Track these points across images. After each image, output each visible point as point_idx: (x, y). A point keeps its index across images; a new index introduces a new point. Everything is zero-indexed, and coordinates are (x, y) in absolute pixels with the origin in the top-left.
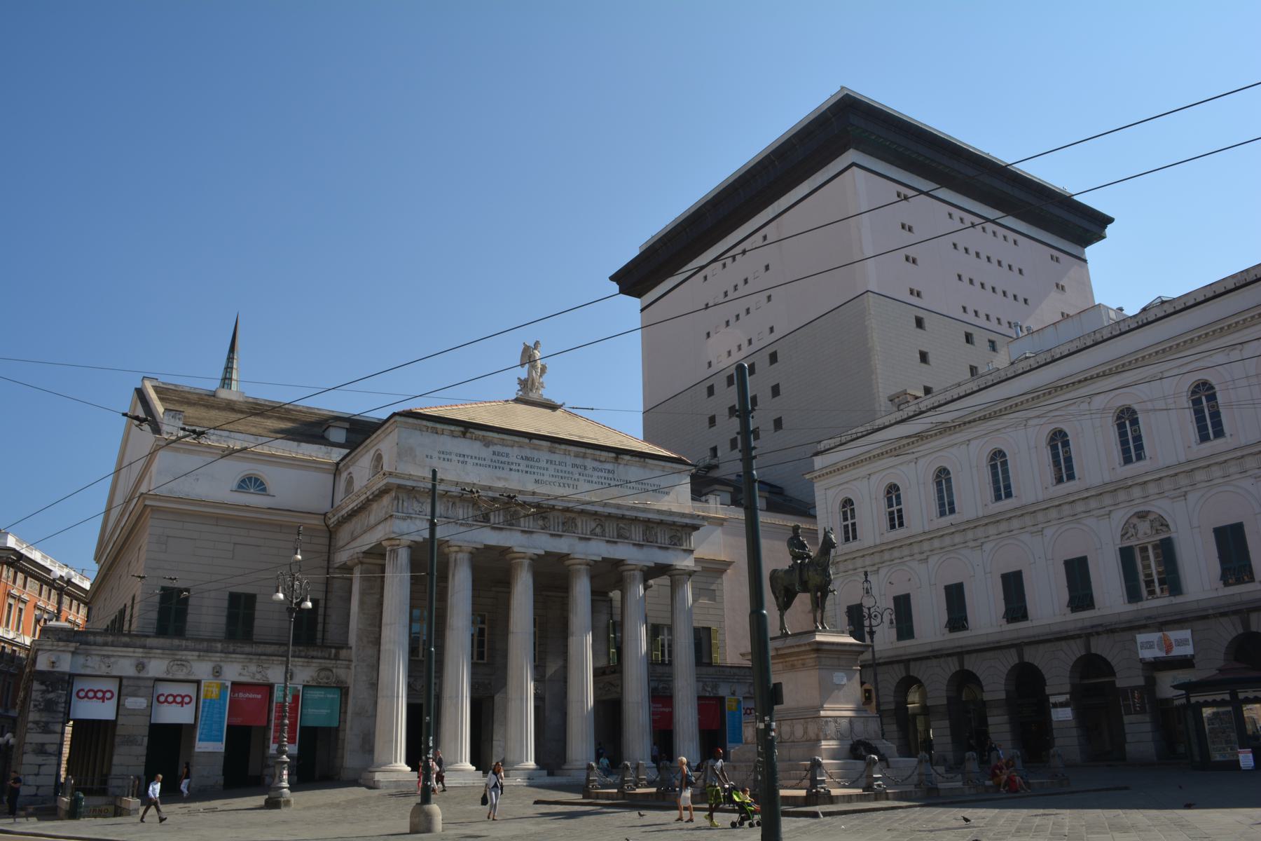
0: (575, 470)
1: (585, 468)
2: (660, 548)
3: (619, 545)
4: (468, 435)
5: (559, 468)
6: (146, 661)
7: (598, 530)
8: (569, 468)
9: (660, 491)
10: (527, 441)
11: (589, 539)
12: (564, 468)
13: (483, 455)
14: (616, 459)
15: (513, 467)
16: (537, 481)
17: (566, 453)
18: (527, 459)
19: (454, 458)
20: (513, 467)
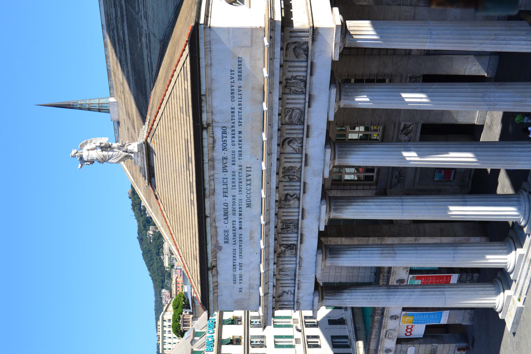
0: (230, 168)
1: (225, 158)
2: (311, 75)
3: (310, 123)
4: (213, 264)
5: (230, 186)
6: (384, 349)
7: (296, 145)
8: (229, 175)
9: (239, 71)
10: (208, 220)
11: (306, 155)
12: (230, 181)
13: (231, 251)
14: (208, 125)
15: (237, 226)
16: (249, 206)
17: (212, 178)
18: (226, 214)
19: (238, 272)
20: (237, 226)
